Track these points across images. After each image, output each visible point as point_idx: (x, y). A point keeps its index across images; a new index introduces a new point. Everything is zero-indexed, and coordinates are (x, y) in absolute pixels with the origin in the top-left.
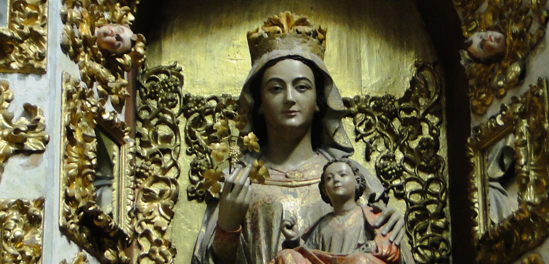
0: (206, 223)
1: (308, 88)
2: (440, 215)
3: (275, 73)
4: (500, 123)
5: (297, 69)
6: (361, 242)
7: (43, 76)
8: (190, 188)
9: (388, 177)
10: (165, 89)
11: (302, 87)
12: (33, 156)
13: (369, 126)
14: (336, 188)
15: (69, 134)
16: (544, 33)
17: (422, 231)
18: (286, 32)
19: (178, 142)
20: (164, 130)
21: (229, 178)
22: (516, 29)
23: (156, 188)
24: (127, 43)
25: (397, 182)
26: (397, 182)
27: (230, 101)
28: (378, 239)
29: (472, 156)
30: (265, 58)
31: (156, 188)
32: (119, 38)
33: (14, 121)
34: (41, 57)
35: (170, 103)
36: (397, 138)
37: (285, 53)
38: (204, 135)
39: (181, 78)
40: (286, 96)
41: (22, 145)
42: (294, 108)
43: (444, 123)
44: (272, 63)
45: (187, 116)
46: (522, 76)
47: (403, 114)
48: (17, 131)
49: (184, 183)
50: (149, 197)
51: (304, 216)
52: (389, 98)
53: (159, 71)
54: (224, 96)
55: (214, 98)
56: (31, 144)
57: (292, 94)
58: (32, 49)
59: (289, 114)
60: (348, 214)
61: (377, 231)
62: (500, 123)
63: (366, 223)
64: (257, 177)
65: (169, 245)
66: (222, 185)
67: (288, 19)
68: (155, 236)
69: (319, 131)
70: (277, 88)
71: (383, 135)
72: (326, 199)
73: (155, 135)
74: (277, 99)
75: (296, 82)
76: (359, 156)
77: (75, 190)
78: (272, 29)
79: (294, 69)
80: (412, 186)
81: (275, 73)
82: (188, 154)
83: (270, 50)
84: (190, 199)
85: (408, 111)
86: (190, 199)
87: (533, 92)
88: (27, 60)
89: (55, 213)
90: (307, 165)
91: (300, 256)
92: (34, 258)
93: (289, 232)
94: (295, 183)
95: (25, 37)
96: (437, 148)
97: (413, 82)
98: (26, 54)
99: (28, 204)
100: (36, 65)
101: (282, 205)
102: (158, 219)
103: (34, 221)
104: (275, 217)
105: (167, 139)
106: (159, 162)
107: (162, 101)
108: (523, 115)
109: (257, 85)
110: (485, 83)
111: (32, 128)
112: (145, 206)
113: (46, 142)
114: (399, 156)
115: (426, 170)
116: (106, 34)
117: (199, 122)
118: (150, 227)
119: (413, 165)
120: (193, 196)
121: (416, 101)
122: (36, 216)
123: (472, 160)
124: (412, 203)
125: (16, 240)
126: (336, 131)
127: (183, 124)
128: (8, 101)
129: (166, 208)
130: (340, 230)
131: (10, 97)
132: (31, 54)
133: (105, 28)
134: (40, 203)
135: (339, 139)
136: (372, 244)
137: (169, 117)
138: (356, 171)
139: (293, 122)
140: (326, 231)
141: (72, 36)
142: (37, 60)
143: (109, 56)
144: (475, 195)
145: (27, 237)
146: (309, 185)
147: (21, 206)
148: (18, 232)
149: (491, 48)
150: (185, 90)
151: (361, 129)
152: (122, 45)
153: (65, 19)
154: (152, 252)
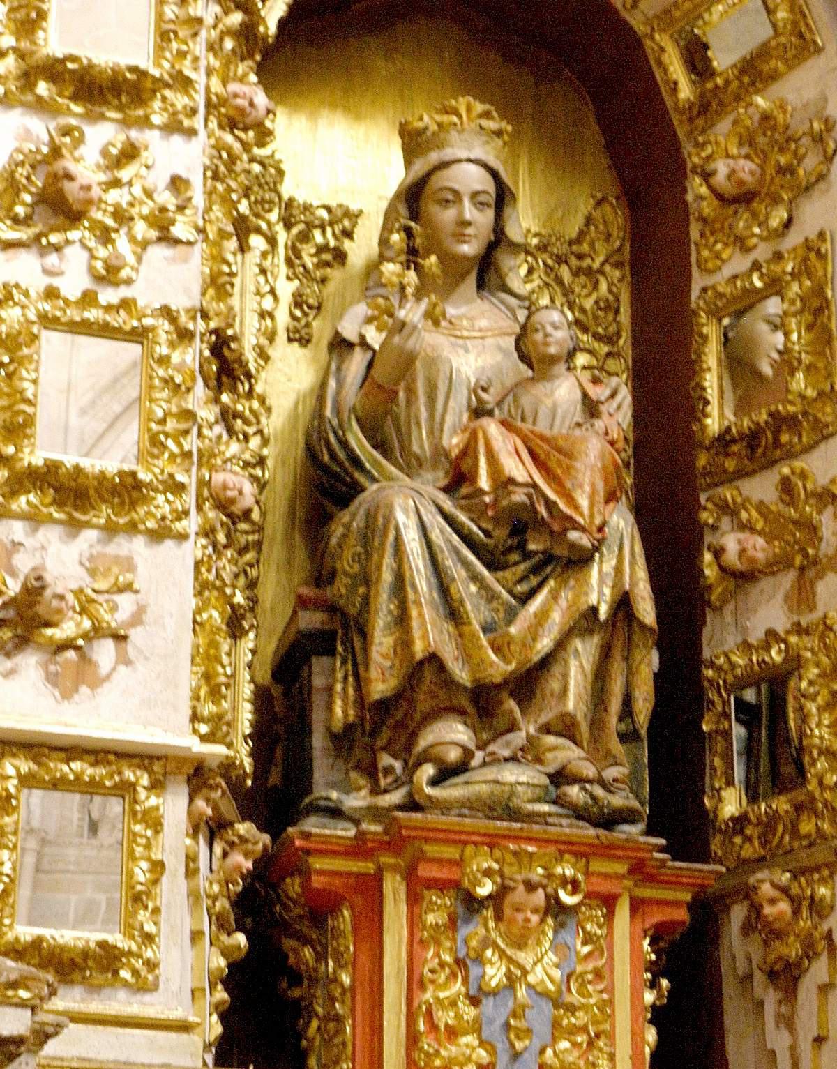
1: (488, 205)
3: (448, 180)
4: (758, 284)
6: (580, 420)
7: (194, 139)
8: (291, 328)
10: (260, 186)
11: (481, 203)
12: (180, 248)
14: (546, 344)
16: (829, 170)
18: (466, 126)
19: (276, 260)
21: (402, 314)
29: (703, 325)
30: (434, 157)
32: (252, 104)
33: (155, 196)
35: (267, 206)
37: (463, 154)
38: (312, 256)
39: (281, 173)
40: (461, 213)
41: (168, 230)
42: (469, 231)
43: (629, 278)
44: (444, 165)
45: (288, 226)
46: (788, 224)
47: (573, 261)
48: (163, 210)
54: (340, 206)
55: (328, 209)
57: (469, 211)
59: (461, 238)
60: (557, 383)
61: (603, 408)
62: (758, 284)
63: (585, 395)
64: (434, 318)
66: (390, 321)
67: (469, 109)
70: (447, 201)
71: (547, 285)
72: (524, 358)
74: (447, 216)
75: (475, 195)
78: (445, 119)
81: (448, 180)
82: (289, 278)
83: (441, 146)
84: (290, 340)
86: (290, 340)
87: (808, 246)
88: (175, 114)
92: (183, 388)
93: (484, 396)
94: (465, 333)
98: (172, 105)
99: (178, 312)
101: (450, 361)
104: (442, 375)
107: (256, 202)
116: (236, 96)
117: (305, 237)
122: (187, 330)
123: (705, 330)
126: (510, 269)
128: (148, 167)
130: (549, 402)
131: (150, 163)
132: (179, 107)
137: (264, 226)
142: (187, 116)
144: (708, 376)
145: (176, 358)
146: (482, 338)
148: (164, 350)
149: (741, 183)
150: (287, 190)
152: (254, 113)
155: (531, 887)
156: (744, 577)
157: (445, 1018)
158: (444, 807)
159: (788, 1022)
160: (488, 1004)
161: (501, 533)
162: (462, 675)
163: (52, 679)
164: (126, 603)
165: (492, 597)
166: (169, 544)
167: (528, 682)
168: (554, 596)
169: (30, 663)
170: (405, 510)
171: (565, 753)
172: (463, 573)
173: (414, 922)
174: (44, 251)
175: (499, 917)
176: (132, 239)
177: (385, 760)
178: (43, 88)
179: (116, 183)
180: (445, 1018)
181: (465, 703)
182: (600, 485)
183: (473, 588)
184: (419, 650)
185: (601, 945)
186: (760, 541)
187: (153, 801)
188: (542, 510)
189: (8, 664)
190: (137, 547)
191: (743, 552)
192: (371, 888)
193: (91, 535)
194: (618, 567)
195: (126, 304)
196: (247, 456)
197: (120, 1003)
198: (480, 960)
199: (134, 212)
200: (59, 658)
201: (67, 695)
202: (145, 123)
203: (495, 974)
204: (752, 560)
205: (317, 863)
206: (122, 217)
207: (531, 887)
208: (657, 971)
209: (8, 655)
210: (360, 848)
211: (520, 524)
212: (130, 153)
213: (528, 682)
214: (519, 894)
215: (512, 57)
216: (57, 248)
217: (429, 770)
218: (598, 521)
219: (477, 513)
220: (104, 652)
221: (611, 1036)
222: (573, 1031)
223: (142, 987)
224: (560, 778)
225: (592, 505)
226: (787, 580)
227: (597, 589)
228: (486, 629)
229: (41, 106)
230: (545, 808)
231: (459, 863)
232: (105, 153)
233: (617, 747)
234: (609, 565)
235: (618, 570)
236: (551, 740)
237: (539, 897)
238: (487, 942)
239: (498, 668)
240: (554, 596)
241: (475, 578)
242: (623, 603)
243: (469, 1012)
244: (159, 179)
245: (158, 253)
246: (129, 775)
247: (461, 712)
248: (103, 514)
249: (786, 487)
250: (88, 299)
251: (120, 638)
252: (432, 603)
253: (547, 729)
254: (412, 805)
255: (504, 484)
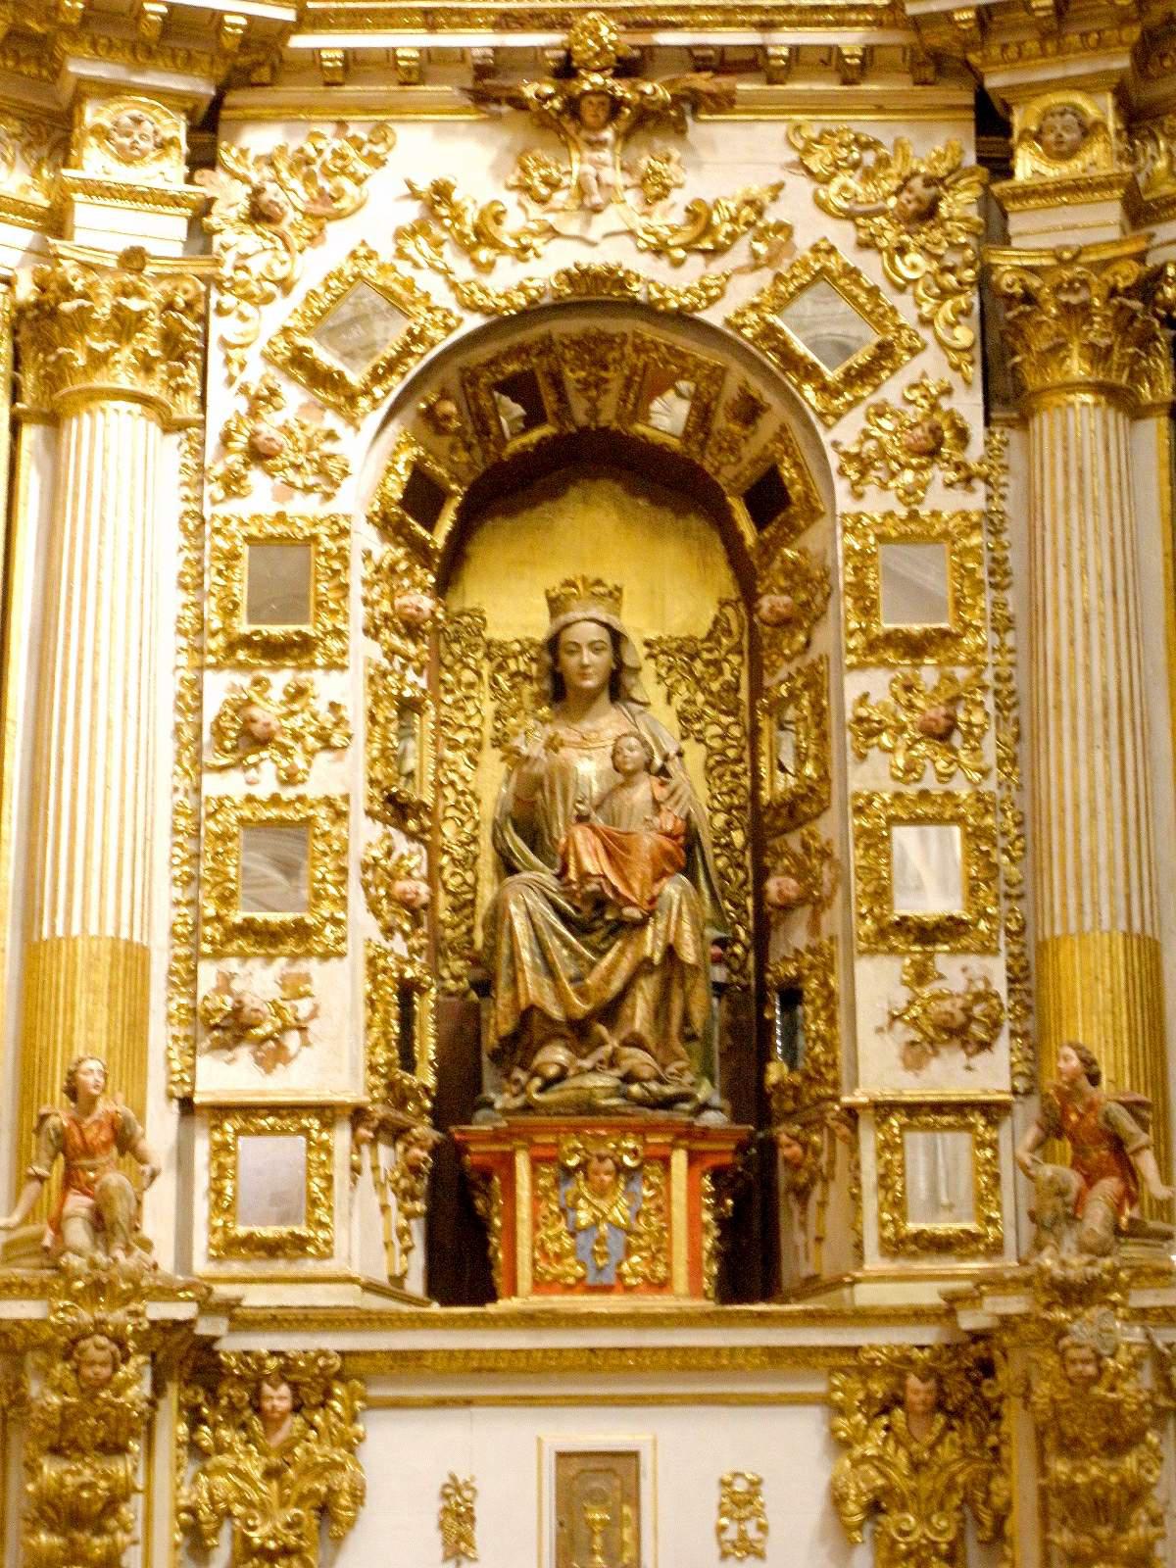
0: (507, 782)
2: (739, 760)
5: (593, 632)
9: (687, 720)
13: (670, 669)
15: (372, 718)
17: (721, 777)
20: (468, 676)
22: (803, 596)
23: (461, 737)
24: (427, 614)
25: (697, 726)
26: (697, 726)
27: (533, 644)
28: (663, 815)
30: (563, 619)
31: (461, 737)
32: (419, 609)
34: (344, 653)
36: (698, 681)
37: (580, 615)
44: (568, 626)
46: (808, 644)
47: (706, 655)
48: (323, 728)
49: (488, 731)
50: (455, 746)
51: (599, 780)
52: (691, 639)
53: (461, 614)
56: (337, 740)
57: (588, 657)
58: (334, 645)
59: (584, 676)
65: (473, 794)
68: (460, 787)
69: (616, 686)
72: (616, 769)
73: (459, 682)
76: (658, 709)
77: (378, 773)
79: (590, 632)
80: (716, 730)
85: (710, 650)
87: (813, 666)
89: (361, 797)
90: (608, 723)
91: (589, 832)
95: (325, 634)
96: (737, 690)
97: (716, 622)
100: (339, 661)
102: (463, 769)
103: (340, 816)
105: (471, 685)
106: (463, 709)
108: (806, 687)
109: (553, 644)
110: (775, 644)
111: (336, 725)
112: (449, 754)
113: (349, 737)
114: (700, 698)
115: (727, 713)
118: (453, 776)
119: (713, 707)
120: (497, 743)
121: (719, 643)
124: (711, 748)
125: (324, 834)
127: (486, 669)
129: (471, 758)
133: (405, 600)
134: (346, 798)
135: (636, 694)
136: (657, 821)
138: (644, 744)
139: (590, 683)
140: (616, 802)
141: (373, 618)
143: (411, 629)
147: (329, 802)
148: (327, 826)
149: (779, 614)
150: (487, 634)
151: (663, 672)
153: (366, 602)
154: (458, 801)
155: (601, 1159)
156: (786, 908)
157: (553, 1247)
158: (546, 1109)
159: (803, 1225)
160: (581, 1237)
161: (587, 909)
162: (557, 1013)
163: (259, 1061)
164: (304, 1007)
165: (576, 955)
166: (334, 961)
167: (611, 1011)
168: (622, 951)
169: (244, 1052)
170: (516, 903)
171: (637, 1059)
172: (558, 943)
173: (534, 1185)
174: (246, 769)
175: (586, 1178)
176: (306, 752)
177: (520, 1075)
178: (241, 655)
179: (293, 713)
180: (553, 1247)
181: (565, 1030)
182: (649, 871)
183: (565, 952)
184: (523, 1003)
185: (664, 1192)
186: (793, 882)
187: (325, 1136)
188: (611, 895)
189: (229, 1055)
190: (312, 966)
191: (780, 893)
192: (508, 1161)
193: (282, 961)
194: (679, 918)
195: (301, 799)
196: (463, 838)
197: (310, 1267)
198: (575, 1208)
199: (304, 732)
200: (264, 1047)
201: (268, 1071)
202: (313, 665)
203: (584, 1217)
204: (788, 898)
205: (472, 1148)
206: (297, 737)
207: (601, 1159)
208: (719, 1197)
209: (230, 1049)
210: (497, 1136)
211: (600, 903)
212: (300, 692)
213: (611, 1011)
214: (594, 1164)
215: (656, 501)
216: (255, 765)
217: (537, 1082)
218: (647, 897)
219: (570, 896)
220: (292, 1040)
221: (669, 1251)
222: (640, 1249)
223: (323, 1256)
224: (629, 1078)
225: (642, 887)
226: (808, 908)
227: (651, 944)
228: (572, 981)
229: (241, 666)
230: (614, 1102)
231: (557, 1145)
232: (286, 692)
233: (680, 1049)
234: (660, 926)
235: (668, 927)
236: (627, 1051)
237: (609, 1164)
238: (578, 1196)
239: (581, 1007)
240: (622, 951)
241: (566, 944)
242: (671, 952)
243: (568, 1242)
244: (321, 706)
245: (323, 758)
246: (304, 1122)
247: (563, 1037)
248: (290, 946)
249: (805, 846)
250: (275, 800)
251: (302, 1029)
252: (535, 968)
253: (625, 1043)
254: (528, 1108)
255: (585, 876)
